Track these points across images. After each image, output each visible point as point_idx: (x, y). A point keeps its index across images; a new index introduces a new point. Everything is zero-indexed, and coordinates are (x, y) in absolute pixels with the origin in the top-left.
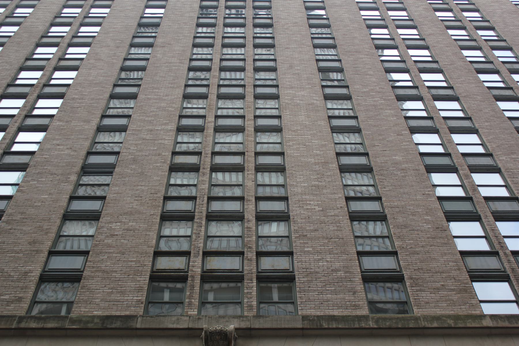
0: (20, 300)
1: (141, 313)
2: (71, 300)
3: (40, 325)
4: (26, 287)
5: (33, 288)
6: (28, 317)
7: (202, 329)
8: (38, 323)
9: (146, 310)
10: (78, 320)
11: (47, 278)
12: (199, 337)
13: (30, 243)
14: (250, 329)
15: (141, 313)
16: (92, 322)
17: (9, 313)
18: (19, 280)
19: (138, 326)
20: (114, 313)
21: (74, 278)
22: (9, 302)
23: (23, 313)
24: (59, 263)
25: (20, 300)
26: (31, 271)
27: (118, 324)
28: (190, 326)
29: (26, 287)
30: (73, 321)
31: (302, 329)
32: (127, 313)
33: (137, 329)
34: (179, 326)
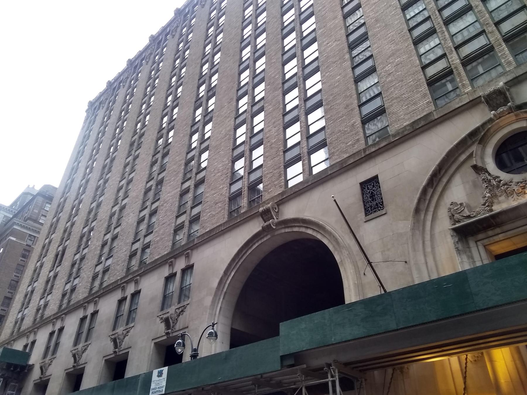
0: (358, 140)
1: (434, 109)
2: (387, 125)
3: (377, 148)
4: (357, 132)
5: (361, 130)
6: (368, 147)
7: (481, 96)
8: (375, 147)
9: (436, 105)
10: (397, 134)
11: (366, 121)
12: (481, 102)
13: (345, 108)
14: (517, 77)
15: (434, 109)
16: (406, 130)
17: (357, 150)
18: (351, 131)
19: (436, 117)
20: (416, 118)
21: (381, 112)
22: (353, 145)
23: (364, 146)
24: (367, 109)
25: (358, 140)
26: (355, 123)
27: (422, 123)
28: (471, 99)
29: (357, 132)
30: (394, 136)
32: (425, 113)
33: (436, 119)
34: (463, 103)
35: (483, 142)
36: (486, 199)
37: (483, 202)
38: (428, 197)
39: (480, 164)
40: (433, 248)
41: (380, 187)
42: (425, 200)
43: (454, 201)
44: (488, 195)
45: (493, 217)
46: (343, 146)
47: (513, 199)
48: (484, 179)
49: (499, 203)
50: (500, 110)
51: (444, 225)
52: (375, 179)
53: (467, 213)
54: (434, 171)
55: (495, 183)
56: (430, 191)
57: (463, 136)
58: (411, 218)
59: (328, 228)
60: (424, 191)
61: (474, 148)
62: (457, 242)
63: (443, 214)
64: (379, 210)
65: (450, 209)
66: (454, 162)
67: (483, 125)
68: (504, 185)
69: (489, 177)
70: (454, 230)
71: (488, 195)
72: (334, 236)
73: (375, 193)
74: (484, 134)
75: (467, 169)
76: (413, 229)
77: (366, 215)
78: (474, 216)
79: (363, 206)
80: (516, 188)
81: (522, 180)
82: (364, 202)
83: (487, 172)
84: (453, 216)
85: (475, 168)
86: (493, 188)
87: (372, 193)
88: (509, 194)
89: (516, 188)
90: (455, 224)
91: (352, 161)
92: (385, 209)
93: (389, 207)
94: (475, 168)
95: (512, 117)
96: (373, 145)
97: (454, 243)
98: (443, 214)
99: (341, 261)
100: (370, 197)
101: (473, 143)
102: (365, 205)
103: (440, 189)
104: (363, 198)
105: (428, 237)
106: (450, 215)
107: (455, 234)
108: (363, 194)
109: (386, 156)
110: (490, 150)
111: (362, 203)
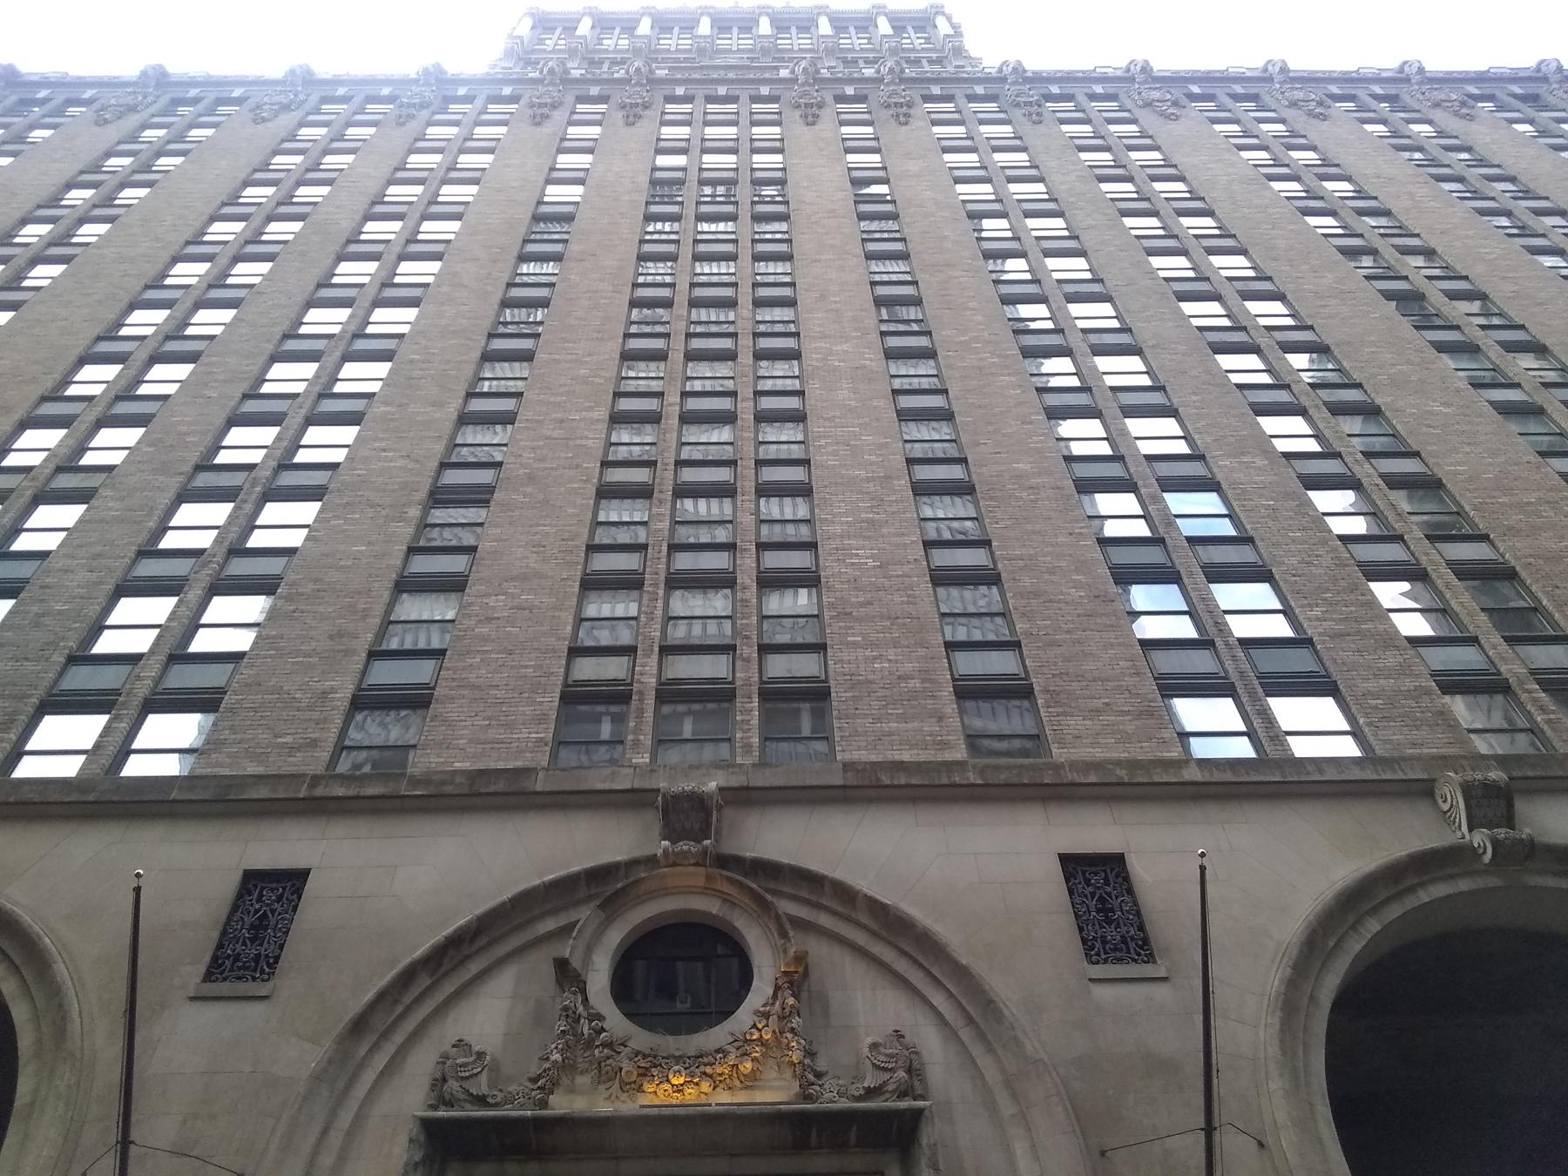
0: (314, 744)
2: (412, 742)
3: (351, 792)
5: (339, 722)
6: (330, 776)
9: (554, 756)
10: (425, 780)
11: (366, 701)
12: (652, 804)
13: (331, 637)
14: (747, 788)
15: (545, 764)
18: (310, 708)
19: (539, 788)
20: (493, 765)
21: (416, 700)
22: (293, 749)
23: (319, 769)
24: (387, 674)
25: (314, 744)
26: (333, 690)
27: (500, 786)
30: (415, 782)
31: (844, 787)
32: (519, 764)
35: (611, 906)
36: (547, 1065)
37: (534, 1070)
38: (408, 999)
39: (576, 963)
40: (342, 1158)
41: (295, 909)
42: (396, 1002)
43: (467, 1038)
44: (556, 1057)
45: (540, 1124)
46: (264, 736)
47: (606, 1094)
48: (566, 1009)
49: (572, 1090)
50: (684, 846)
51: (409, 1097)
52: (295, 880)
53: (482, 1086)
54: (460, 928)
55: (586, 1031)
56: (424, 981)
57: (576, 868)
58: (328, 1043)
59: (61, 970)
60: (408, 976)
61: (584, 913)
62: (416, 1164)
63: (422, 1064)
64: (254, 979)
65: (446, 1057)
66: (521, 927)
67: (633, 863)
68: (604, 1045)
69: (581, 1008)
70: (428, 1125)
71: (556, 1057)
72: (61, 1006)
73: (273, 921)
74: (623, 889)
75: (540, 965)
76: (317, 1078)
77: (208, 977)
78: (496, 1105)
79: (214, 946)
80: (626, 1066)
81: (648, 1052)
82: (224, 933)
83: (583, 991)
84: (444, 1080)
85: (562, 966)
86: (578, 1042)
87: (262, 918)
88: (606, 1075)
89: (626, 1066)
90: (435, 1108)
91: (262, 792)
92: (269, 985)
93: (289, 982)
94: (562, 966)
95: (697, 876)
96: (345, 779)
97: (407, 1164)
98: (422, 1064)
99: (32, 1104)
100: (252, 927)
101: (589, 899)
102: (220, 946)
103: (449, 988)
104: (229, 919)
105: (345, 1118)
106: (438, 1075)
107: (422, 1138)
108: (235, 908)
109: (362, 826)
110: (615, 937)
111: (215, 935)
